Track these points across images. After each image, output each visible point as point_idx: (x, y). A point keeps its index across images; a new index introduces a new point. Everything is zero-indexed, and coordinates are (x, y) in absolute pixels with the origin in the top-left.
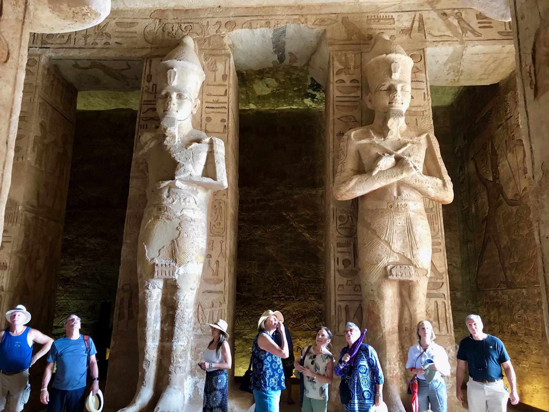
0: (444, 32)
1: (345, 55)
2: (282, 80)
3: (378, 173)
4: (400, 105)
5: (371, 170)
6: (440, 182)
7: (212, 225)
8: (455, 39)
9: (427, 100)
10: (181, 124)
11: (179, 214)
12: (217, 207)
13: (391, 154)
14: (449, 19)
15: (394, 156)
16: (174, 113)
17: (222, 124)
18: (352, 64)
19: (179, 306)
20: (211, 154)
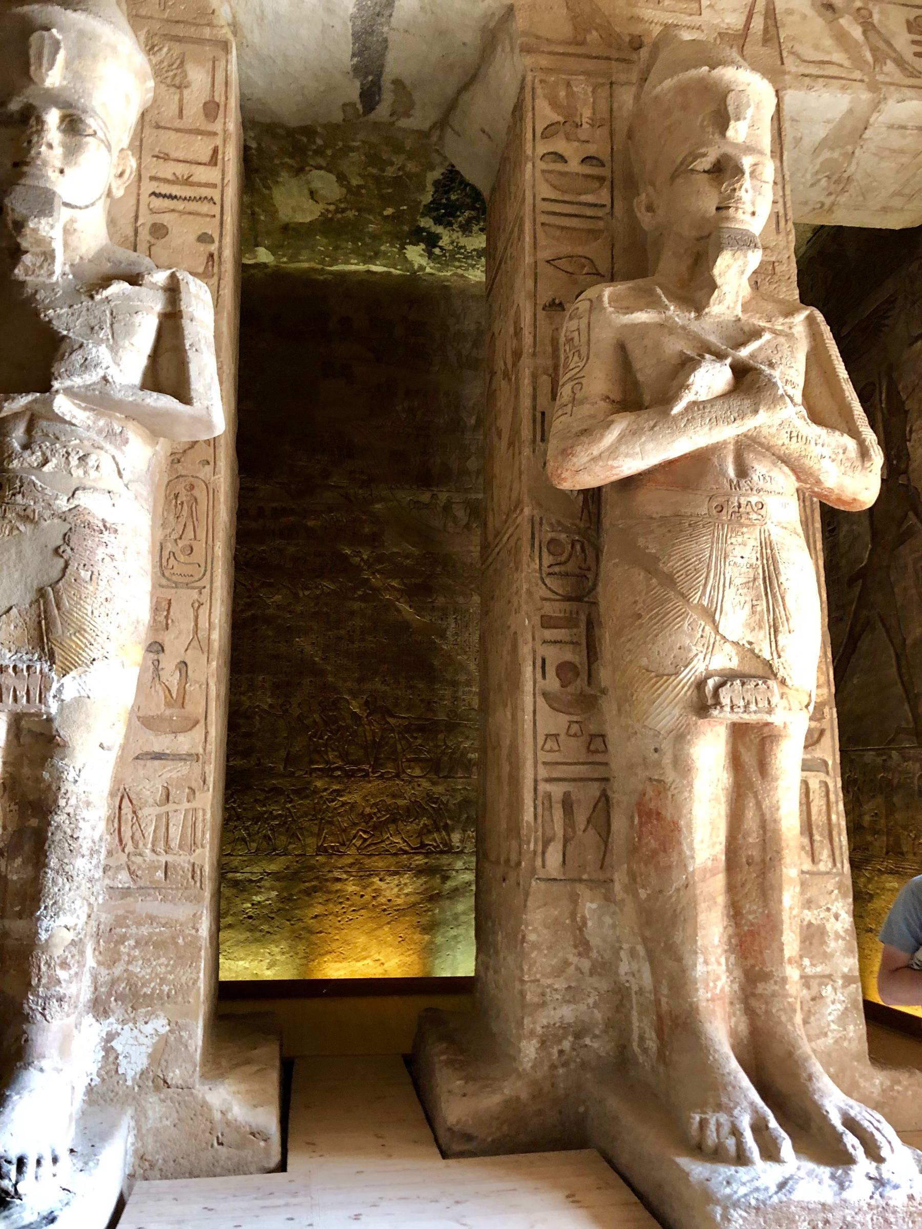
0: (829, 53)
1: (568, 85)
2: (355, 181)
3: (687, 409)
4: (747, 217)
5: (666, 399)
6: (851, 444)
7: (166, 554)
8: (857, 75)
9: (783, 234)
10: (73, 221)
11: (62, 504)
12: (183, 498)
13: (720, 356)
14: (842, 21)
15: (729, 361)
16: (53, 175)
17: (202, 247)
18: (587, 113)
19: (62, 803)
20: (171, 323)
